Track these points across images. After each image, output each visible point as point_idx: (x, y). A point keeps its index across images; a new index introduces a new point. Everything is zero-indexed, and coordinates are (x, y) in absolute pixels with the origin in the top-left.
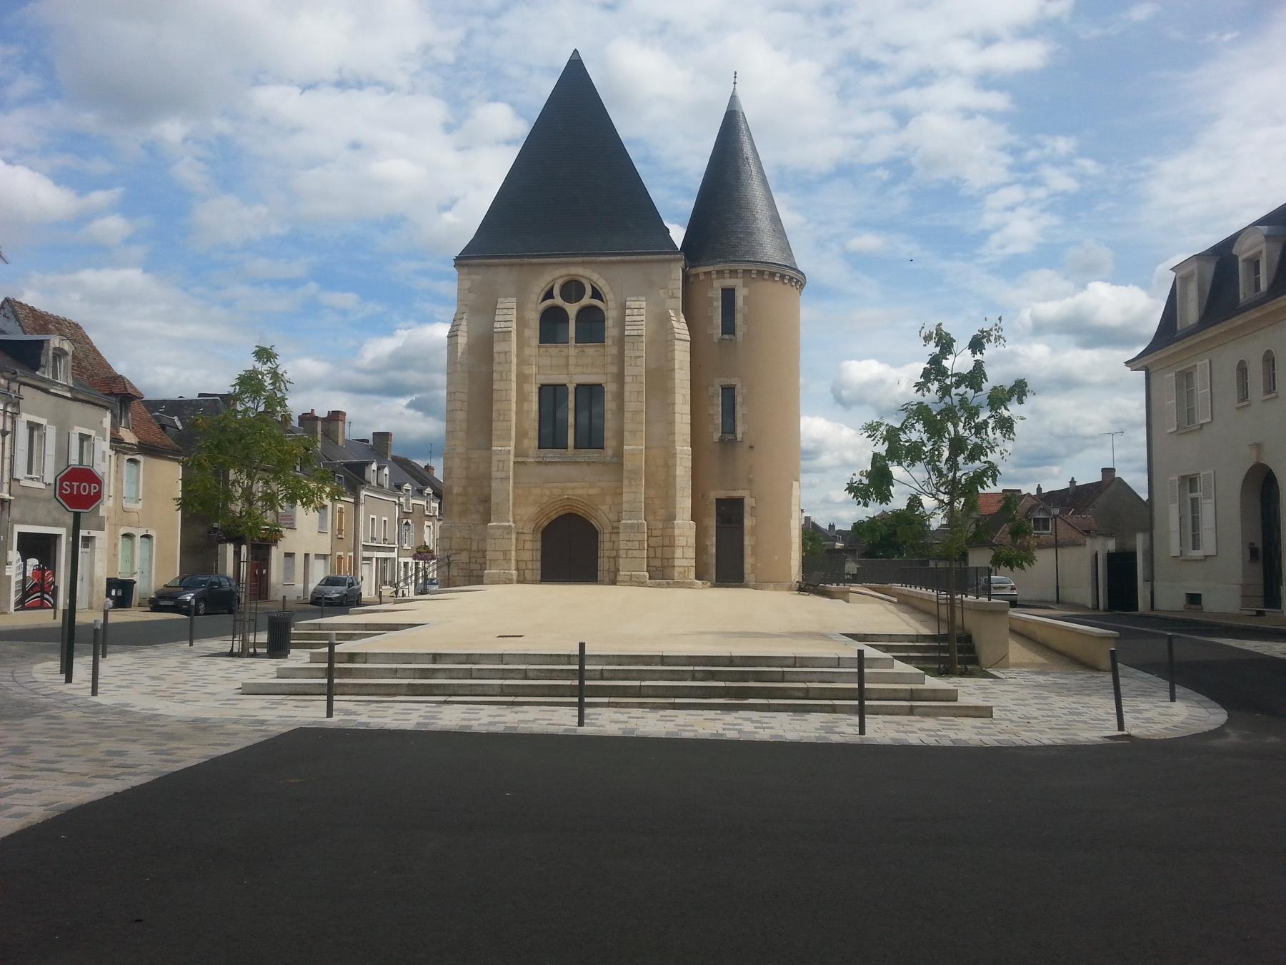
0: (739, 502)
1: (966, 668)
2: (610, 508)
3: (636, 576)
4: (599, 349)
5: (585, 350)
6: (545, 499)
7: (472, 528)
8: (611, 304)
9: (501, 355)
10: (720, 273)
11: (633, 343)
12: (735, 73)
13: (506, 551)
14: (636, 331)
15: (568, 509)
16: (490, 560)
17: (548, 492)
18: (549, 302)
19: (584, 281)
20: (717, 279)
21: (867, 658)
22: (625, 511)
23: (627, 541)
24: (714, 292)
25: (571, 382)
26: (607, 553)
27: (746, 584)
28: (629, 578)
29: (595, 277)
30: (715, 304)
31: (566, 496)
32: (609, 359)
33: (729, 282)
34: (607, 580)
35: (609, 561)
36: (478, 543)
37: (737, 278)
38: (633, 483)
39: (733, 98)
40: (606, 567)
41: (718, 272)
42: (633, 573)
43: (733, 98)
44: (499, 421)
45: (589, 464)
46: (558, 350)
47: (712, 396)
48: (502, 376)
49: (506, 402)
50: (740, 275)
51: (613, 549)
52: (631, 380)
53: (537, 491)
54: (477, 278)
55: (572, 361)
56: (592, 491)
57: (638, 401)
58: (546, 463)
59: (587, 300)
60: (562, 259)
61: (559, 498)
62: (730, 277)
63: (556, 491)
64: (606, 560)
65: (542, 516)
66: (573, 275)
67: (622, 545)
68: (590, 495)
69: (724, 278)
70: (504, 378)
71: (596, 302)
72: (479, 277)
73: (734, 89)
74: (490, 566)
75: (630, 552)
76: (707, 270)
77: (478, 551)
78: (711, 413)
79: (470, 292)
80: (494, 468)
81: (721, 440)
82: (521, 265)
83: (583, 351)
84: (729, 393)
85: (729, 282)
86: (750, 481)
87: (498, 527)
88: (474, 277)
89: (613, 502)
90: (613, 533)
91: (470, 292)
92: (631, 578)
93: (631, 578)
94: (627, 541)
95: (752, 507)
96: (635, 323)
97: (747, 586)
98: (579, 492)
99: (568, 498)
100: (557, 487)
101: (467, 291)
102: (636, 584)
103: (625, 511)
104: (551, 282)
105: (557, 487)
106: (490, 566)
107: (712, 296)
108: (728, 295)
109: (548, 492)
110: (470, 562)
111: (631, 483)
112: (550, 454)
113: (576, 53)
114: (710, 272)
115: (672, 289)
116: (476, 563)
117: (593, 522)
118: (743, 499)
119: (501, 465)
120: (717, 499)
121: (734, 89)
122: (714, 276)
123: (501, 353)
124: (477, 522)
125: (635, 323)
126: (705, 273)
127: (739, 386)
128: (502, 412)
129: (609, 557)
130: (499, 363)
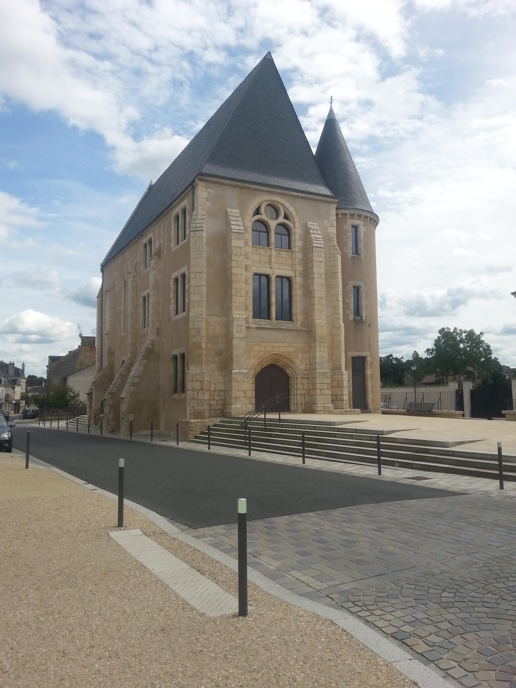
0: (363, 359)
1: (170, 433)
2: (301, 361)
3: (327, 407)
4: (289, 253)
5: (281, 253)
6: (262, 354)
7: (211, 374)
8: (298, 225)
9: (237, 249)
10: (352, 215)
11: (318, 252)
12: (331, 97)
13: (245, 391)
14: (319, 245)
15: (274, 361)
16: (235, 398)
17: (263, 349)
18: (257, 217)
19: (280, 207)
20: (350, 219)
21: (503, 456)
22: (318, 363)
23: (321, 383)
24: (347, 227)
25: (273, 274)
26: (299, 392)
27: (370, 411)
28: (323, 408)
29: (287, 205)
30: (348, 234)
31: (275, 353)
32: (297, 261)
33: (357, 222)
34: (300, 410)
35: (301, 397)
36: (215, 385)
37: (361, 220)
38: (322, 345)
39: (331, 112)
40: (299, 401)
41: (365, 216)
42: (325, 405)
43: (331, 112)
44: (236, 296)
45: (288, 330)
46: (264, 250)
47: (348, 292)
48: (238, 264)
49: (241, 283)
50: (362, 219)
51: (303, 389)
52: (318, 277)
53: (256, 348)
54: (212, 191)
55: (273, 259)
56: (291, 350)
57: (322, 291)
58: (262, 329)
59: (281, 219)
60: (269, 189)
61: (271, 353)
62: (357, 219)
63: (269, 349)
64: (299, 396)
65: (260, 365)
66: (273, 201)
67: (318, 386)
68: (289, 353)
69: (354, 219)
70: (240, 266)
71: (286, 221)
72: (214, 191)
73: (331, 106)
74: (235, 401)
75: (322, 391)
76: (344, 212)
77: (215, 391)
78: (348, 302)
79: (207, 200)
80: (235, 330)
81: (355, 320)
82: (242, 188)
83: (279, 254)
84: (357, 289)
85: (357, 222)
86: (370, 346)
87: (239, 374)
88: (210, 190)
89: (303, 357)
90: (303, 378)
91: (207, 200)
92: (325, 408)
93: (325, 408)
94: (321, 383)
95: (371, 363)
96: (318, 239)
97: (370, 412)
98: (283, 349)
99: (277, 354)
100: (269, 346)
101: (205, 199)
102: (328, 412)
103: (318, 363)
104: (260, 203)
105: (269, 346)
106: (235, 401)
107: (347, 229)
108: (355, 228)
109: (263, 349)
110: (210, 400)
111: (320, 345)
112: (264, 323)
113: (269, 54)
114: (346, 214)
115: (331, 221)
116: (214, 400)
117: (288, 371)
118: (366, 357)
119: (240, 329)
120: (352, 357)
121: (331, 106)
122: (348, 217)
123: (237, 247)
124: (214, 370)
125: (318, 239)
126: (342, 214)
127: (363, 287)
128: (238, 290)
129: (301, 395)
130: (236, 255)
